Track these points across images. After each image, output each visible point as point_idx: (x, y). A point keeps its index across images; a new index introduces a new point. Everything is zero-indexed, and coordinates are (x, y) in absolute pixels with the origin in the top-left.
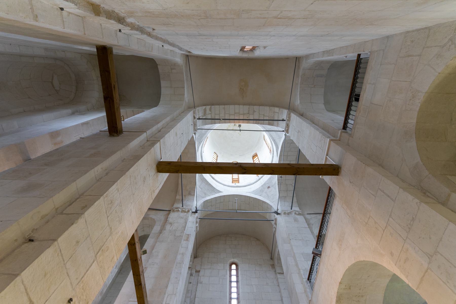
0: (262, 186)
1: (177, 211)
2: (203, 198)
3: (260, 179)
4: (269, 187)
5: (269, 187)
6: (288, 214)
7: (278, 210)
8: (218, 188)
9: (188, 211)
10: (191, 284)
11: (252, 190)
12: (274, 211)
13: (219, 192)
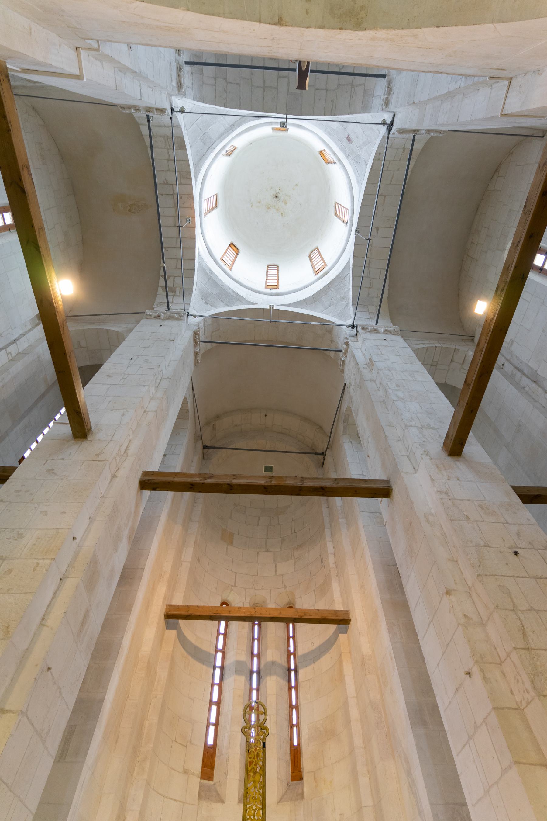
0: (347, 157)
1: (343, 366)
2: (348, 304)
3: (339, 160)
4: (349, 139)
5: (349, 139)
6: (390, 89)
7: (384, 123)
9: (347, 344)
10: (507, 364)
11: (357, 185)
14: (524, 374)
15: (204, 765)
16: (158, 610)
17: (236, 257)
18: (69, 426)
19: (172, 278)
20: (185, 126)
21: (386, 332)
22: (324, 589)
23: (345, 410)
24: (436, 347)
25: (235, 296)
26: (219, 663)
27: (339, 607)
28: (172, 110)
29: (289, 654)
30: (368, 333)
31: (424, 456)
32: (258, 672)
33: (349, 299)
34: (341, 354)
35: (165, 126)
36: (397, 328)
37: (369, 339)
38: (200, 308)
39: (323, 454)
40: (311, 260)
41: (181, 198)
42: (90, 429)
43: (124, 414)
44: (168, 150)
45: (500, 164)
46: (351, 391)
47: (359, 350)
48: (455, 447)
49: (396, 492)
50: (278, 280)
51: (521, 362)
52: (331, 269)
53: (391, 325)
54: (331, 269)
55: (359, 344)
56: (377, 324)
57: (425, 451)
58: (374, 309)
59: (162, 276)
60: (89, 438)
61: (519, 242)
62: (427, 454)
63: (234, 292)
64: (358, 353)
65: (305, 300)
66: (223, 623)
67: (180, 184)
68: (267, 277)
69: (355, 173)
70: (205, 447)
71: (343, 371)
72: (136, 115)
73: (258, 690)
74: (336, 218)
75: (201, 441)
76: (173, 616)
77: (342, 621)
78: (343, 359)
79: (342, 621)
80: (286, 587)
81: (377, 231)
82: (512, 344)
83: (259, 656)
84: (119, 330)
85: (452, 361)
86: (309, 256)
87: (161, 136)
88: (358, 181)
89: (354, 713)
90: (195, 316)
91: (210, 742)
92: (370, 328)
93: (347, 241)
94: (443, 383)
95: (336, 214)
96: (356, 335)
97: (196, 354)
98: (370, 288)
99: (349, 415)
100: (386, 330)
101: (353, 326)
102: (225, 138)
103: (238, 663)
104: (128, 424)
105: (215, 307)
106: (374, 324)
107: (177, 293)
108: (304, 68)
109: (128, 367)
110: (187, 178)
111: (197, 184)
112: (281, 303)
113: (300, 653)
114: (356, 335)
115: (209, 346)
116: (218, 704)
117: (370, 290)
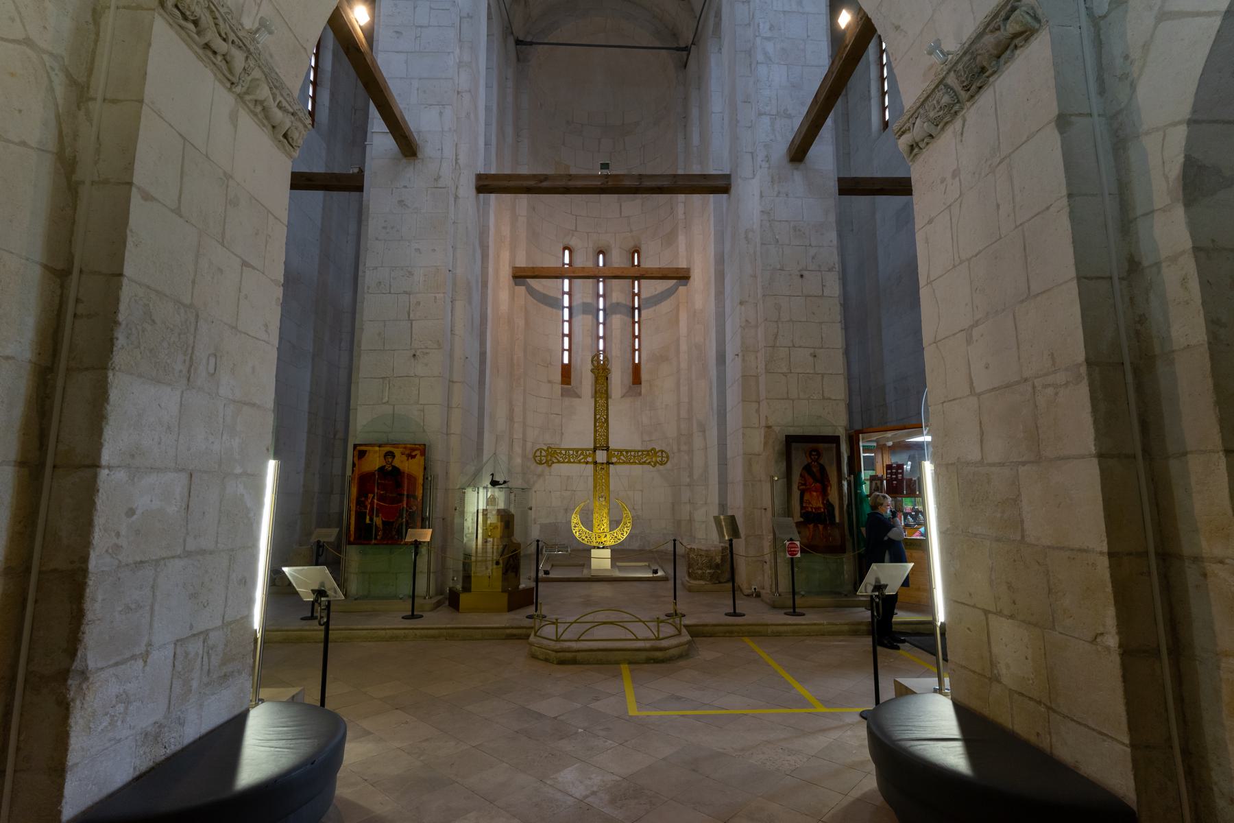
15: (563, 375)
16: (506, 273)
22: (670, 239)
26: (566, 303)
27: (683, 265)
29: (634, 295)
32: (604, 310)
39: (687, 49)
43: (441, 113)
48: (799, 153)
49: (733, 190)
60: (420, 155)
66: (566, 282)
70: (518, 42)
73: (604, 324)
76: (520, 276)
77: (683, 276)
79: (683, 276)
80: (631, 231)
83: (604, 296)
89: (684, 347)
91: (566, 361)
103: (585, 304)
113: (643, 296)
116: (569, 336)
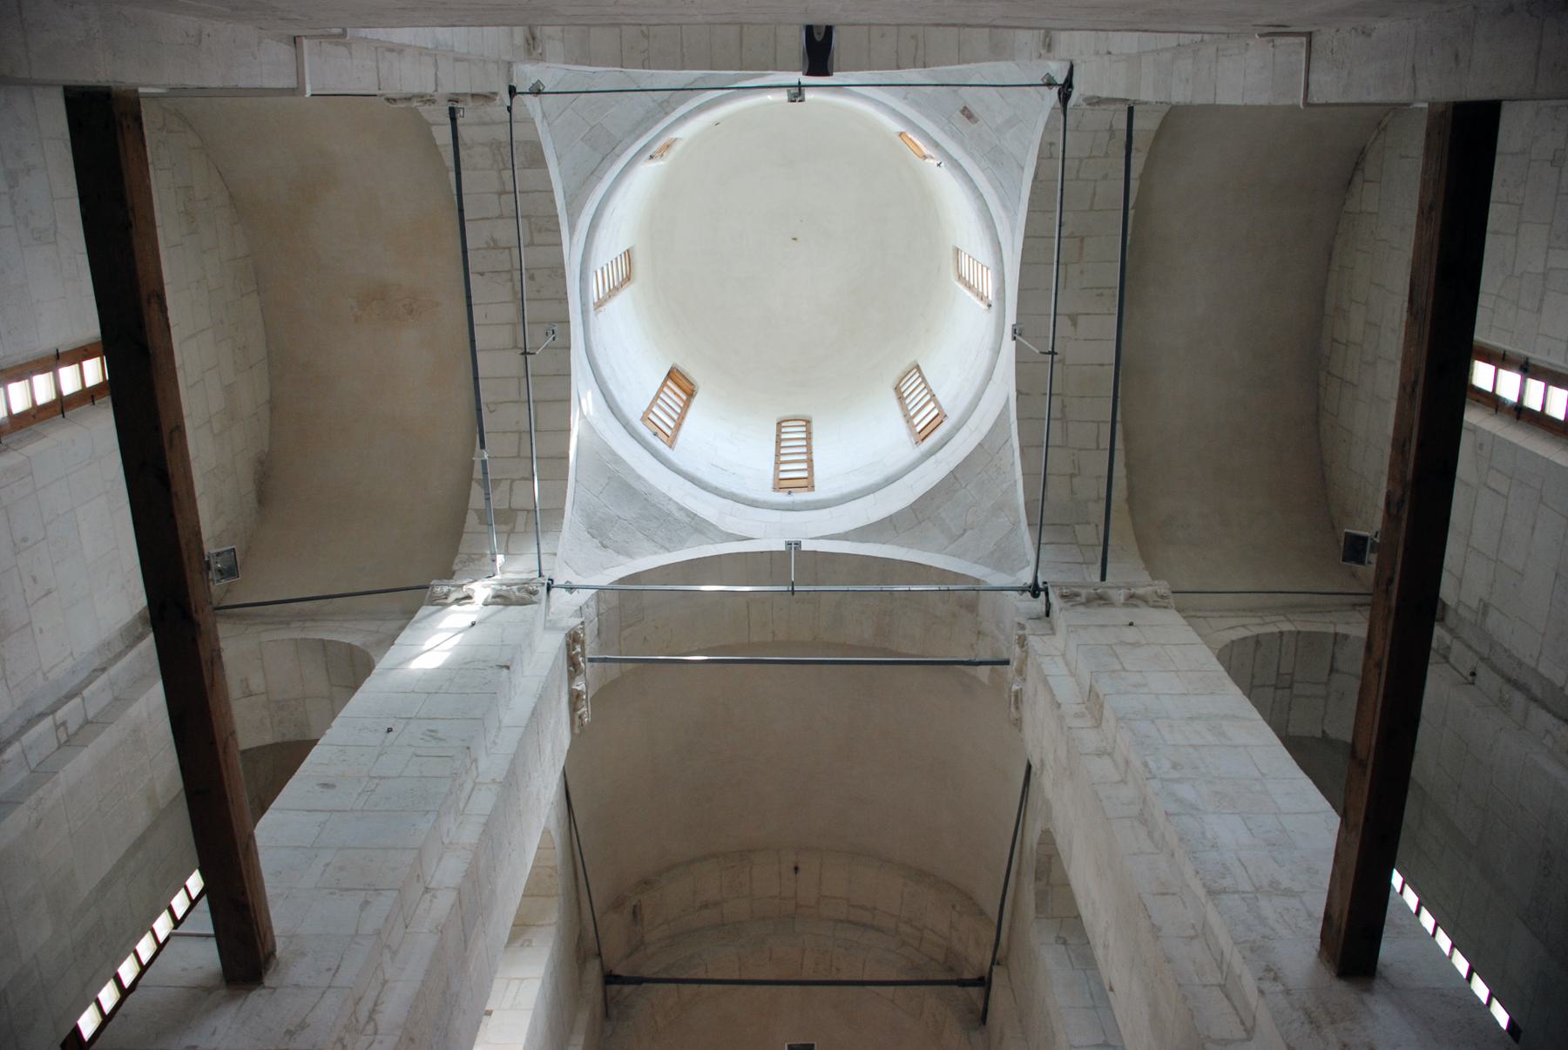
2: (1016, 523)
8: (985, 429)
9: (1022, 641)
12: (1059, 105)
13: (1002, 417)
14: (1534, 699)
17: (687, 404)
18: (213, 944)
19: (505, 486)
20: (544, 116)
21: (1133, 601)
23: (1035, 841)
24: (1281, 633)
25: (687, 520)
28: (512, 91)
30: (1081, 609)
31: (1266, 985)
33: (1017, 510)
34: (1010, 671)
35: (493, 123)
36: (1163, 587)
37: (1085, 627)
38: (583, 566)
39: (984, 982)
40: (901, 398)
41: (532, 278)
42: (272, 953)
43: (367, 903)
44: (500, 171)
45: (1363, 152)
46: (1046, 782)
47: (1059, 660)
50: (810, 461)
51: (1520, 664)
52: (957, 428)
53: (1145, 577)
54: (957, 428)
55: (1058, 641)
56: (1103, 578)
57: (1268, 969)
58: (1091, 534)
59: (478, 481)
61: (1415, 382)
62: (1275, 979)
63: (682, 509)
64: (1055, 670)
65: (890, 519)
67: (531, 244)
68: (778, 455)
69: (995, 188)
70: (610, 979)
71: (1018, 723)
72: (425, 111)
74: (961, 286)
75: (597, 962)
78: (1015, 688)
81: (1075, 324)
82: (1485, 614)
84: (356, 640)
85: (1332, 670)
86: (897, 389)
87: (482, 144)
88: (1004, 206)
90: (571, 588)
92: (1083, 592)
93: (997, 351)
94: (1319, 735)
95: (960, 277)
96: (1048, 614)
97: (575, 699)
98: (1072, 476)
99: (1050, 857)
100: (1132, 596)
101: (1035, 590)
102: (647, 130)
104: (378, 933)
105: (630, 555)
106: (1096, 578)
107: (520, 526)
108: (819, 38)
109: (380, 755)
110: (548, 230)
111: (575, 238)
112: (817, 531)
114: (1048, 614)
115: (614, 671)
117: (1076, 481)
